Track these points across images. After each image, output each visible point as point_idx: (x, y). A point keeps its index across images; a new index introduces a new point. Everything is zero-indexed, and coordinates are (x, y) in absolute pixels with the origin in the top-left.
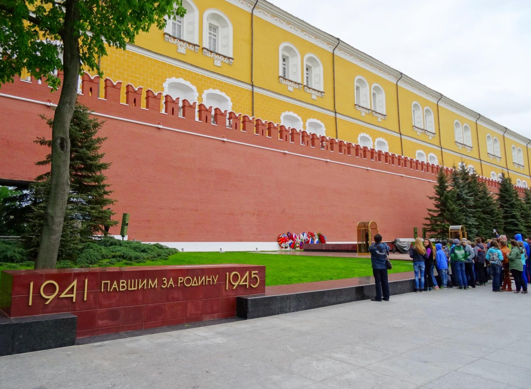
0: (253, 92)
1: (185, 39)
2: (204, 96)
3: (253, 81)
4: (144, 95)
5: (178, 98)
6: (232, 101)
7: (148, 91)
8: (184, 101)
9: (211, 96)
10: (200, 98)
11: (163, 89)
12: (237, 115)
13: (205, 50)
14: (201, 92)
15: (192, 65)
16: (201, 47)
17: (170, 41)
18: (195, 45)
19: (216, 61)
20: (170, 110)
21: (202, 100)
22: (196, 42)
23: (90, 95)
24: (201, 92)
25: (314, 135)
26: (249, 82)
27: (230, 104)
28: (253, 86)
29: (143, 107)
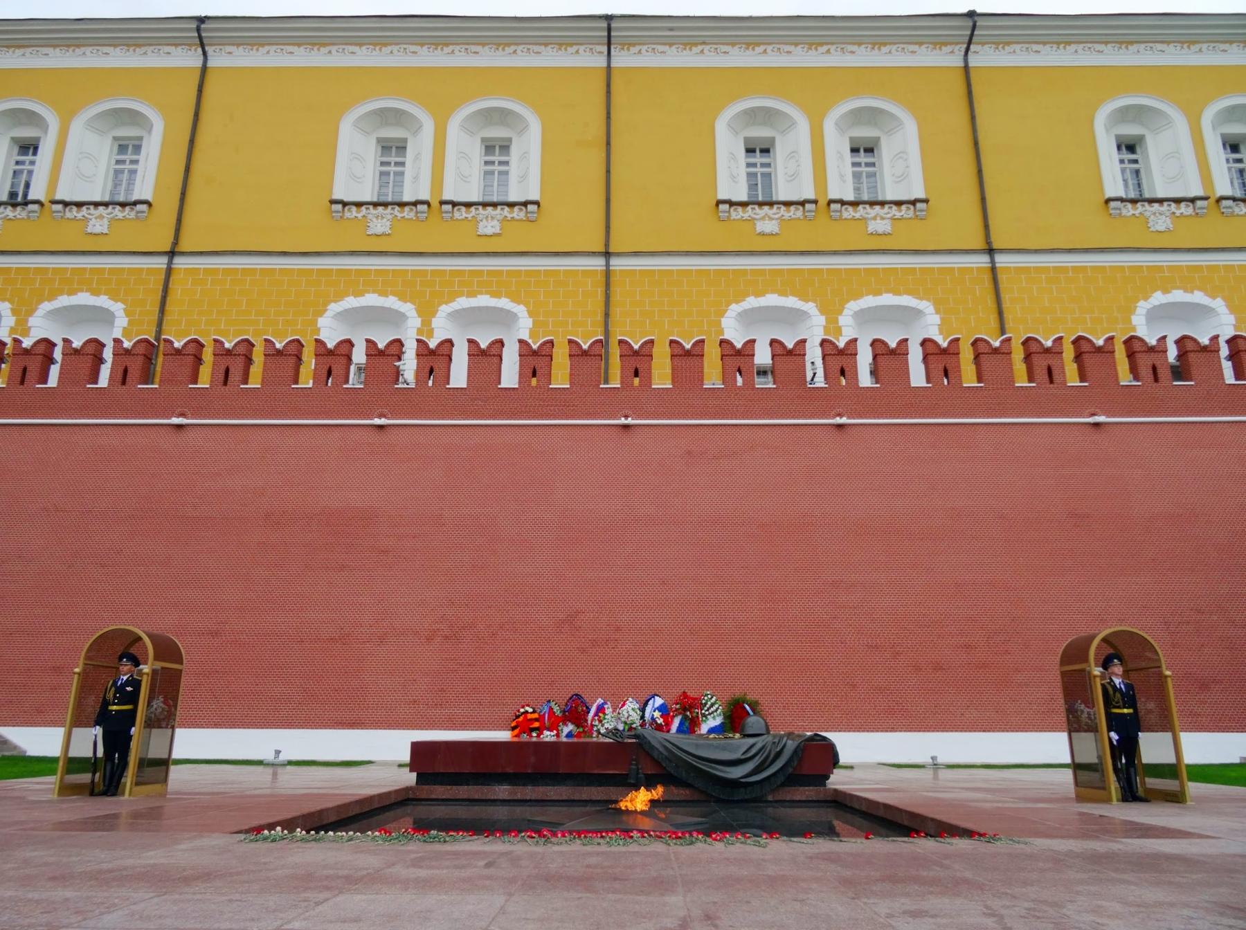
1: (1160, 194)
4: (1069, 352)
7: (1026, 342)
8: (1180, 342)
13: (1225, 203)
15: (1189, 250)
16: (1212, 200)
17: (1124, 212)
18: (1193, 200)
20: (1145, 372)
22: (1197, 191)
23: (843, 382)
29: (1073, 380)
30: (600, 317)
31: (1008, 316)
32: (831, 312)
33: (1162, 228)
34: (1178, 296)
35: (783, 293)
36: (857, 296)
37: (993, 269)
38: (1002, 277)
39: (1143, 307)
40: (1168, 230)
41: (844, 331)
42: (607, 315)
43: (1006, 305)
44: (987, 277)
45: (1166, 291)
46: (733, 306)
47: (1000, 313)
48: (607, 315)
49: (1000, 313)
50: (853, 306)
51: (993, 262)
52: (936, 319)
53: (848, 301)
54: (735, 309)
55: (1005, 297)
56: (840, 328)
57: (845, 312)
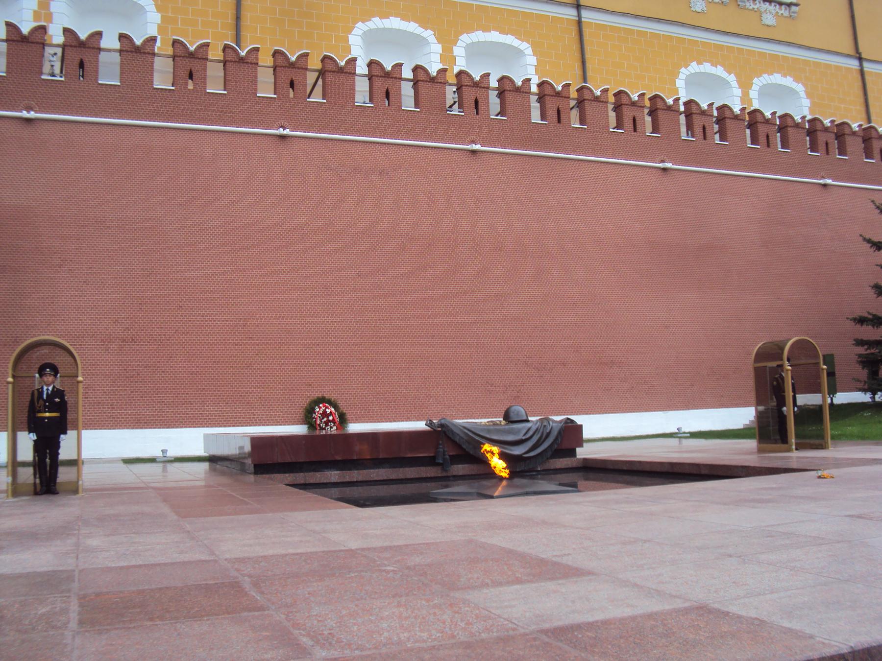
0: (862, 73)
2: (753, 94)
3: (861, 50)
5: (712, 104)
6: (809, 95)
9: (767, 92)
10: (745, 97)
11: (676, 91)
12: (635, 97)
14: (745, 86)
19: (764, 15)
21: (750, 101)
24: (745, 86)
25: (785, 117)
26: (852, 52)
27: (806, 102)
28: (860, 59)
30: (231, 21)
31: (589, 65)
32: (448, 42)
33: (699, 10)
34: (707, 68)
35: (404, 18)
36: (470, 30)
37: (579, 23)
38: (586, 31)
39: (684, 72)
40: (702, 12)
41: (458, 60)
42: (238, 18)
43: (588, 56)
44: (574, 29)
45: (699, 63)
46: (360, 25)
47: (583, 63)
48: (238, 18)
49: (583, 63)
50: (466, 39)
51: (579, 15)
52: (532, 60)
53: (462, 34)
54: (360, 28)
55: (588, 48)
56: (454, 58)
57: (459, 43)
